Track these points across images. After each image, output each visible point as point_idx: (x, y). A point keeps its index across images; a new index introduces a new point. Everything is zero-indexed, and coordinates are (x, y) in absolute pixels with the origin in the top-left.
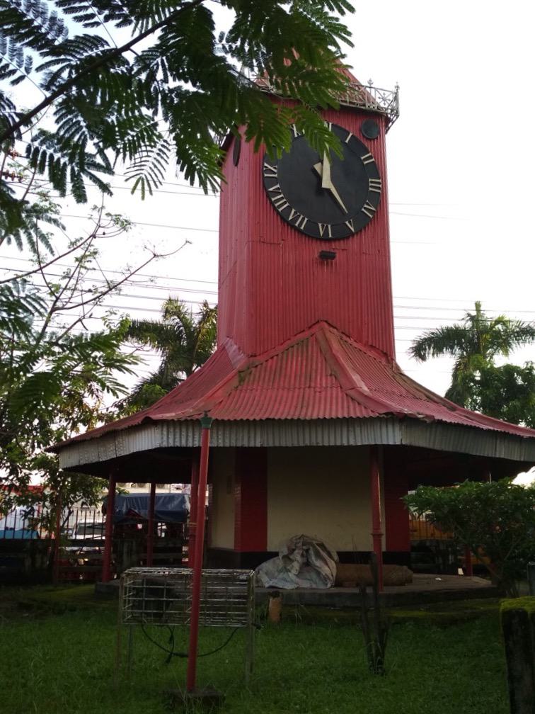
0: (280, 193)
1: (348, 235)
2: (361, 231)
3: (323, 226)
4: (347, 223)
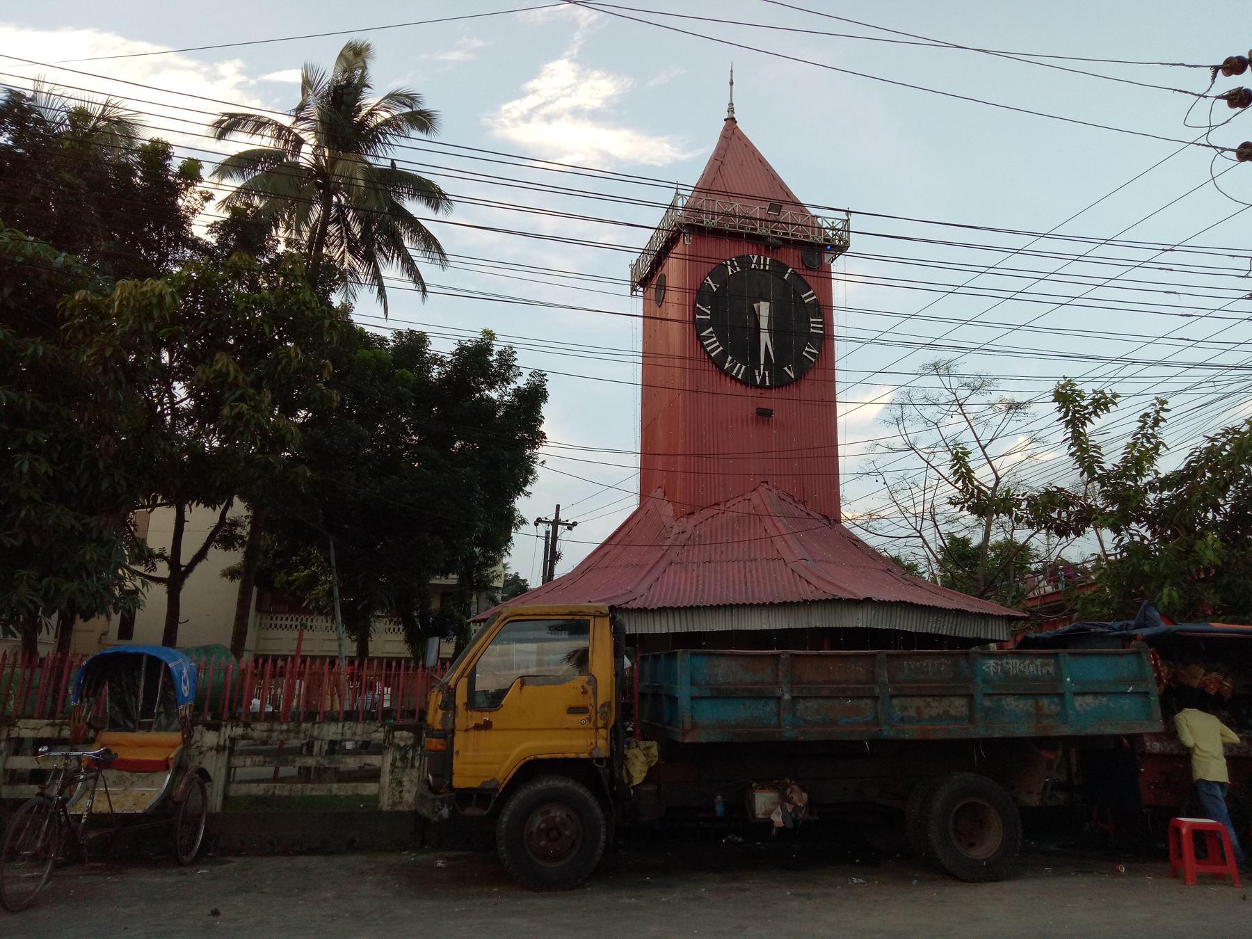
2: (801, 378)
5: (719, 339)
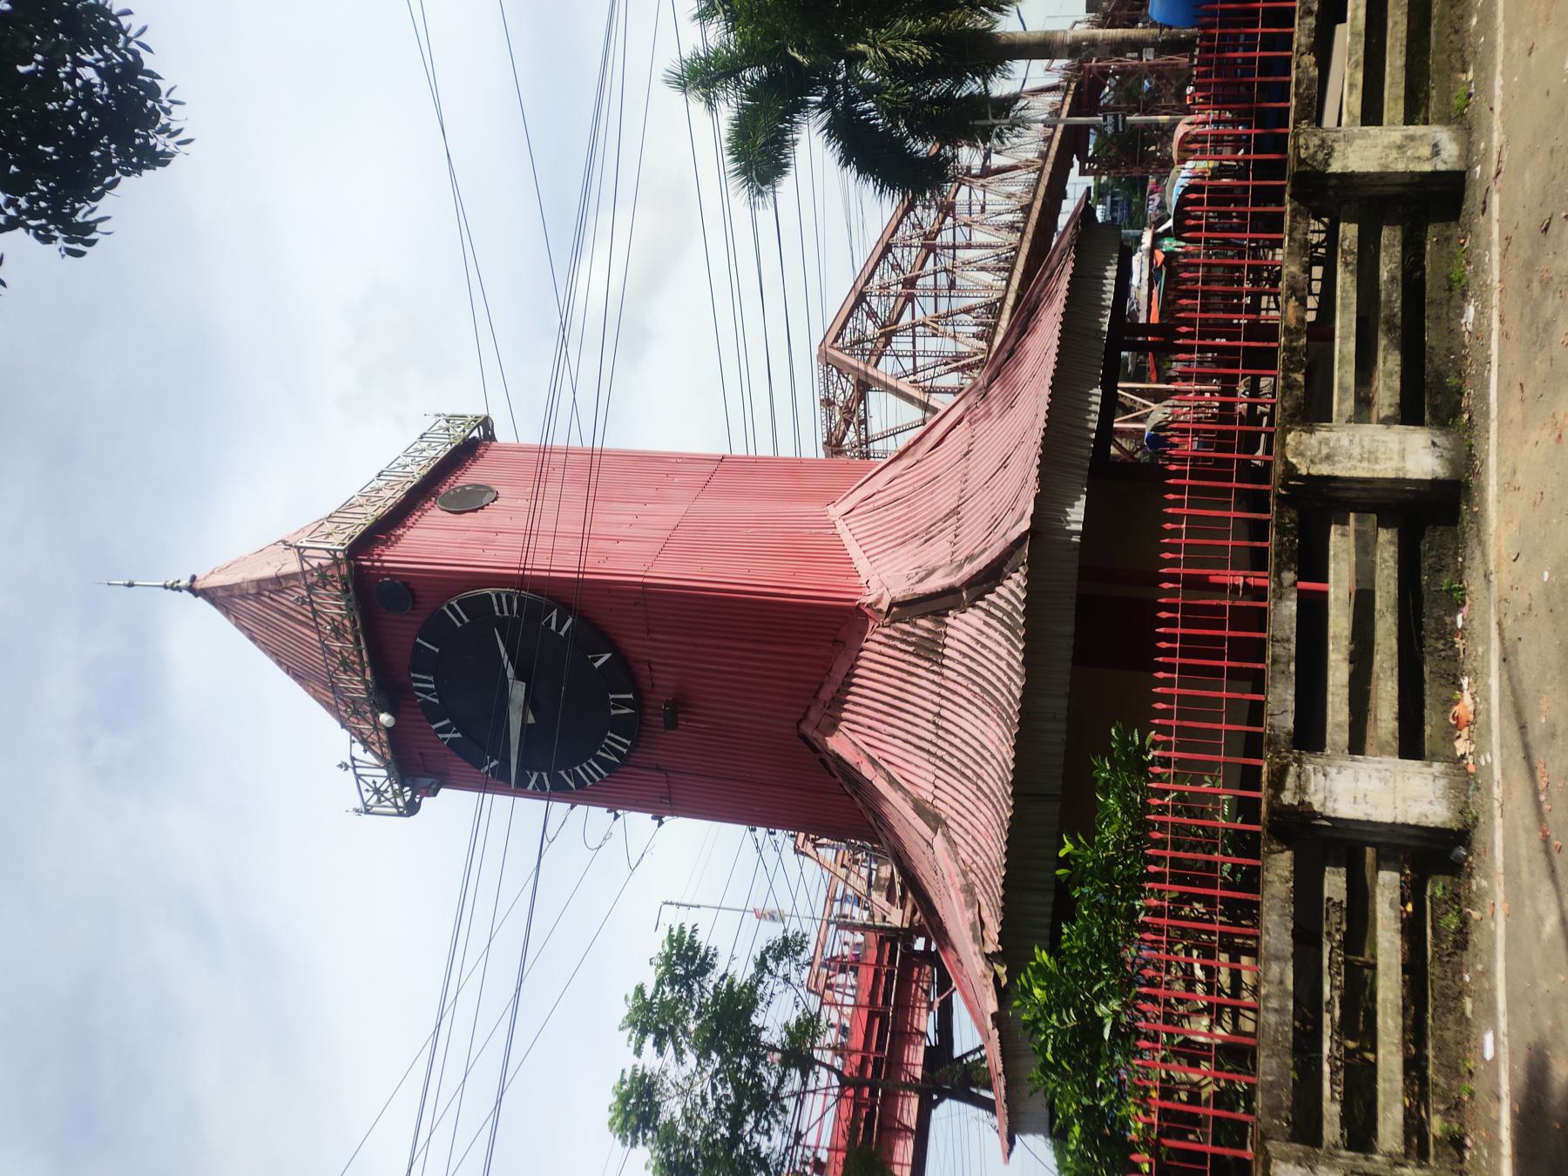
0: (575, 772)
1: (622, 660)
3: (615, 708)
5: (580, 763)
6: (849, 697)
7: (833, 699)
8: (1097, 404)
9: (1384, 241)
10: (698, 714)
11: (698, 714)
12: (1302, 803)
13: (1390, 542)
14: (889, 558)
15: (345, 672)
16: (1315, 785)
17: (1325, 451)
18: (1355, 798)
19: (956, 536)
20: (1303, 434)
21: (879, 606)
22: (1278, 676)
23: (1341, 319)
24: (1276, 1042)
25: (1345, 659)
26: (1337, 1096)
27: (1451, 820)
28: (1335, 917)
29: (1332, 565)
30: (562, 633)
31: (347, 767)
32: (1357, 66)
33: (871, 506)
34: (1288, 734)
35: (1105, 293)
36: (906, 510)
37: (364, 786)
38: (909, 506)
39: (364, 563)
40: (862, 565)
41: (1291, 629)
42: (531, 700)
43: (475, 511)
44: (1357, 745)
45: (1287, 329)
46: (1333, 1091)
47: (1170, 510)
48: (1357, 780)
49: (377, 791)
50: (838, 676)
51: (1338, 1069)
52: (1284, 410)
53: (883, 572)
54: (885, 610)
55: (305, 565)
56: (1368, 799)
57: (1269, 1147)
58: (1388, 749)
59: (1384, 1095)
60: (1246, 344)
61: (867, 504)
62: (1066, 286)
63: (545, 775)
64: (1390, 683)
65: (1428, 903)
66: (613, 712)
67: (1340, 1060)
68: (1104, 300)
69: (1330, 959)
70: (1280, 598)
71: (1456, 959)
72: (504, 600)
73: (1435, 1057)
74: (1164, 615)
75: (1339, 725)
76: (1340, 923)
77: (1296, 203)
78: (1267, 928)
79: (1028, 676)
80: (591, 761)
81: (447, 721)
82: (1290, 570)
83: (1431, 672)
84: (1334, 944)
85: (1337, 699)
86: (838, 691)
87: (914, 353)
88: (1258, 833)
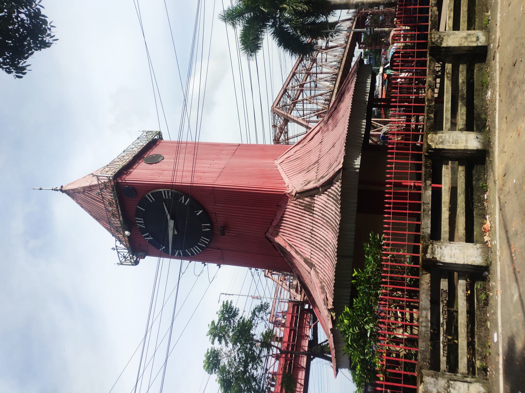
0: (191, 250)
1: (206, 212)
3: (204, 229)
4: (198, 214)
6: (282, 224)
7: (277, 225)
8: (364, 125)
9: (460, 69)
10: (231, 230)
11: (231, 230)
12: (433, 258)
13: (463, 171)
14: (295, 178)
15: (113, 218)
16: (438, 252)
17: (441, 140)
18: (451, 256)
19: (318, 170)
20: (434, 135)
21: (292, 194)
22: (425, 216)
23: (446, 96)
24: (425, 337)
25: (448, 210)
26: (445, 355)
27: (483, 263)
28: (444, 295)
29: (443, 178)
30: (186, 204)
31: (114, 249)
32: (451, 11)
33: (289, 160)
34: (429, 235)
35: (367, 88)
36: (301, 161)
37: (120, 256)
38: (302, 160)
39: (119, 181)
40: (286, 180)
41: (429, 200)
42: (176, 227)
43: (156, 163)
44: (452, 238)
45: (428, 99)
46: (444, 353)
47: (389, 161)
48: (451, 250)
49: (125, 257)
50: (279, 217)
51: (446, 346)
52: (427, 127)
53: (294, 182)
54: (294, 195)
55: (99, 182)
56: (455, 256)
57: (422, 372)
58: (462, 239)
59: (461, 354)
60: (414, 104)
61: (288, 160)
62: (354, 86)
63: (181, 251)
64: (462, 218)
65: (475, 291)
66: (203, 230)
67: (446, 343)
68: (367, 90)
69: (443, 309)
70: (426, 190)
71: (484, 309)
72: (166, 193)
73: (478, 341)
74: (387, 196)
75: (445, 232)
76: (446, 297)
77: (431, 57)
78: (422, 299)
79: (342, 216)
80: (196, 246)
81: (148, 234)
82: (429, 180)
83: (476, 214)
84: (444, 304)
85: (445, 223)
86: (279, 222)
87: (303, 109)
88: (418, 268)
